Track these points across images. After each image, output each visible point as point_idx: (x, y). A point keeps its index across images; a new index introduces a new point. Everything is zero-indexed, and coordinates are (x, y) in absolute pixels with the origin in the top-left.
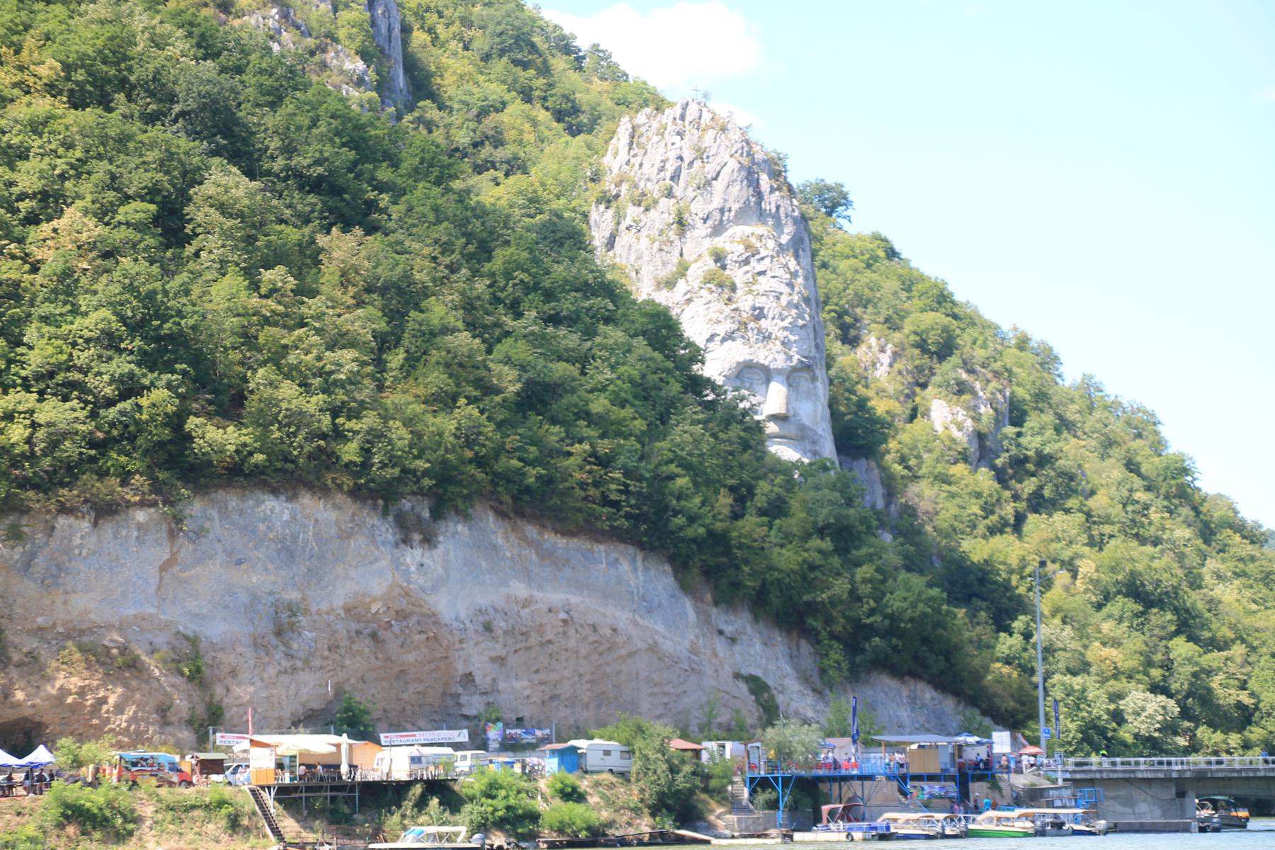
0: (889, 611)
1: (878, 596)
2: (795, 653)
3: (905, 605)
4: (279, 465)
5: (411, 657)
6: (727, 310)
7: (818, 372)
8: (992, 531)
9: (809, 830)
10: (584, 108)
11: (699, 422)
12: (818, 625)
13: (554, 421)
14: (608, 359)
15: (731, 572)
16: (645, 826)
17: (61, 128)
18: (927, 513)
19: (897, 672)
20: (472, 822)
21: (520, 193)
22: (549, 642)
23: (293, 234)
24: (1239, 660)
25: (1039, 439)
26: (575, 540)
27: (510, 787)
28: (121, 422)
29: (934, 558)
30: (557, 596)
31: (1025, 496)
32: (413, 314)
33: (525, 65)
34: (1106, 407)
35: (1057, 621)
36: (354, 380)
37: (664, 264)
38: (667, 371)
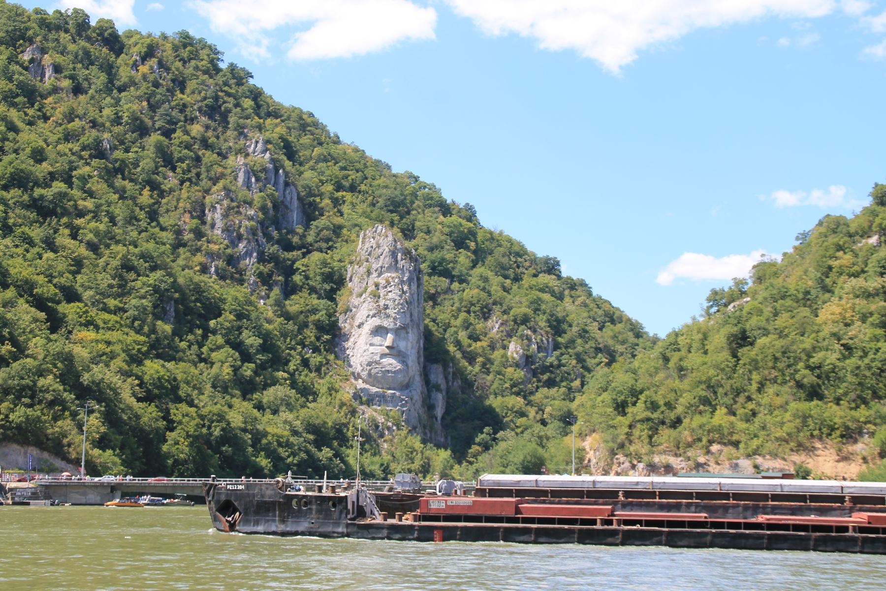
7: (410, 330)
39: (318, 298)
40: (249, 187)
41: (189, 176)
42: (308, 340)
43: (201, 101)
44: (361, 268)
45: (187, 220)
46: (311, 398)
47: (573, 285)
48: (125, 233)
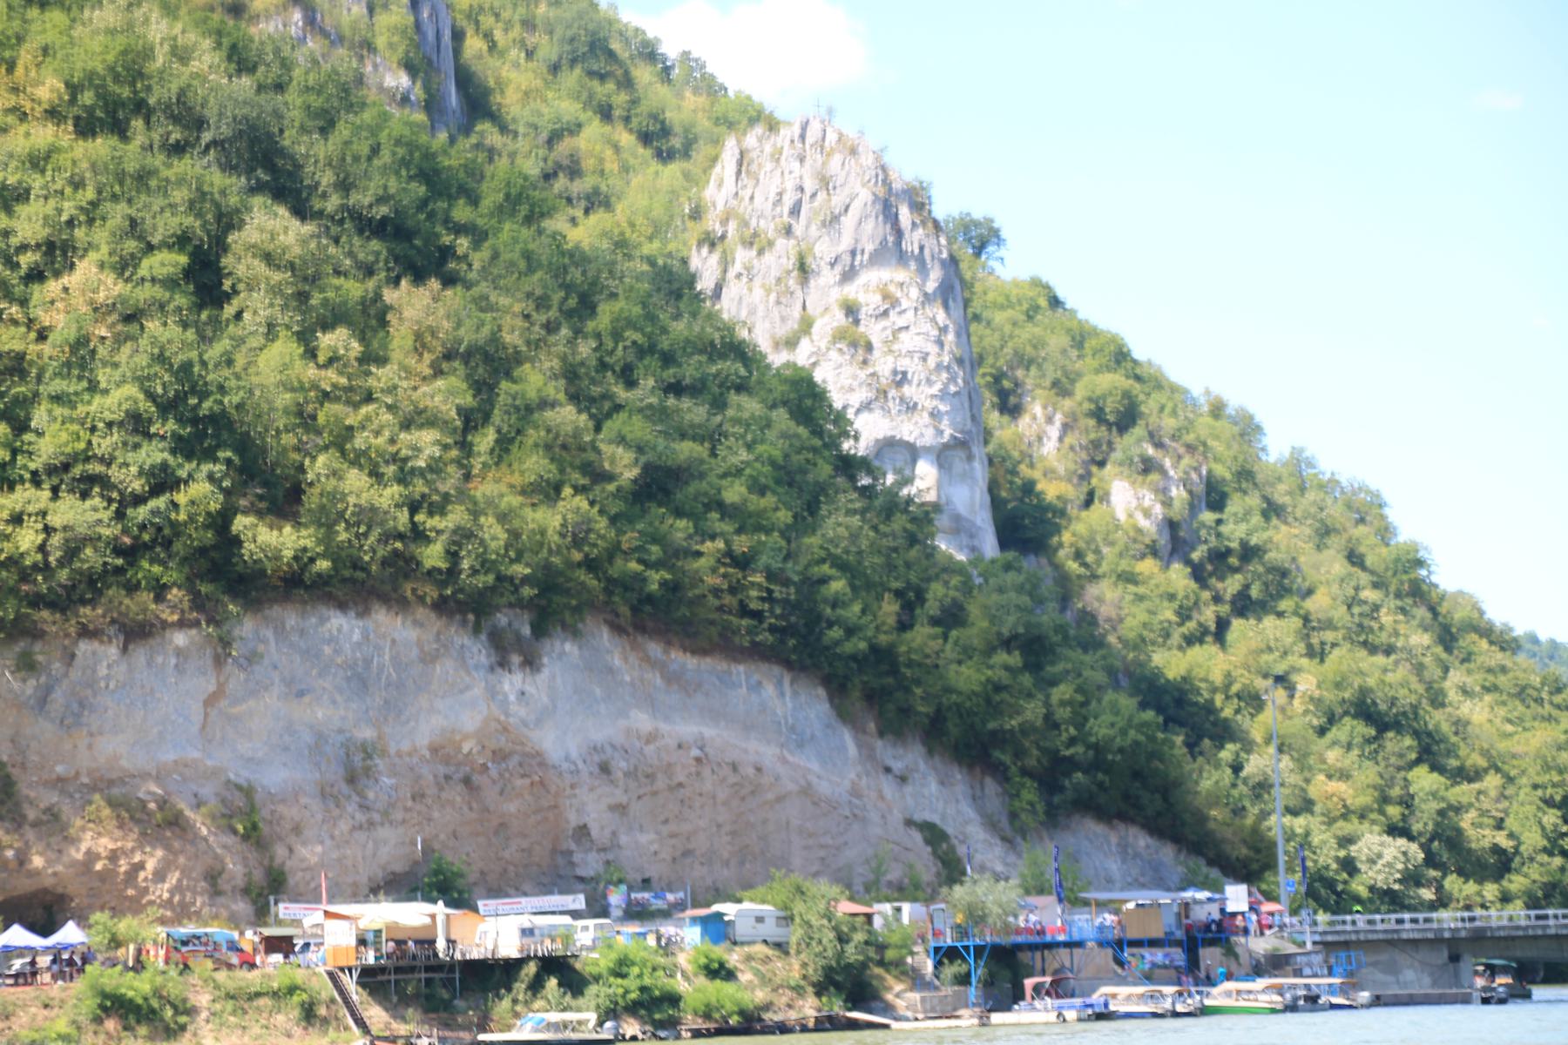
0: (1093, 739)
1: (1080, 721)
2: (978, 793)
3: (1111, 732)
4: (347, 573)
5: (512, 807)
6: (862, 374)
8: (1190, 640)
9: (1008, 1009)
10: (677, 129)
11: (855, 512)
12: (1006, 758)
13: (679, 513)
14: (743, 436)
15: (899, 695)
16: (809, 1008)
17: (69, 164)
18: (1109, 620)
19: (1105, 815)
20: (598, 1007)
21: (604, 234)
22: (680, 785)
23: (355, 289)
24: (1493, 793)
25: (1243, 527)
26: (708, 660)
27: (644, 963)
28: (152, 524)
29: (1120, 676)
30: (688, 729)
31: (1228, 597)
32: (504, 385)
33: (602, 77)
34: (1321, 486)
35: (1272, 750)
36: (435, 467)
37: (783, 319)
38: (814, 450)
44: (768, 257)
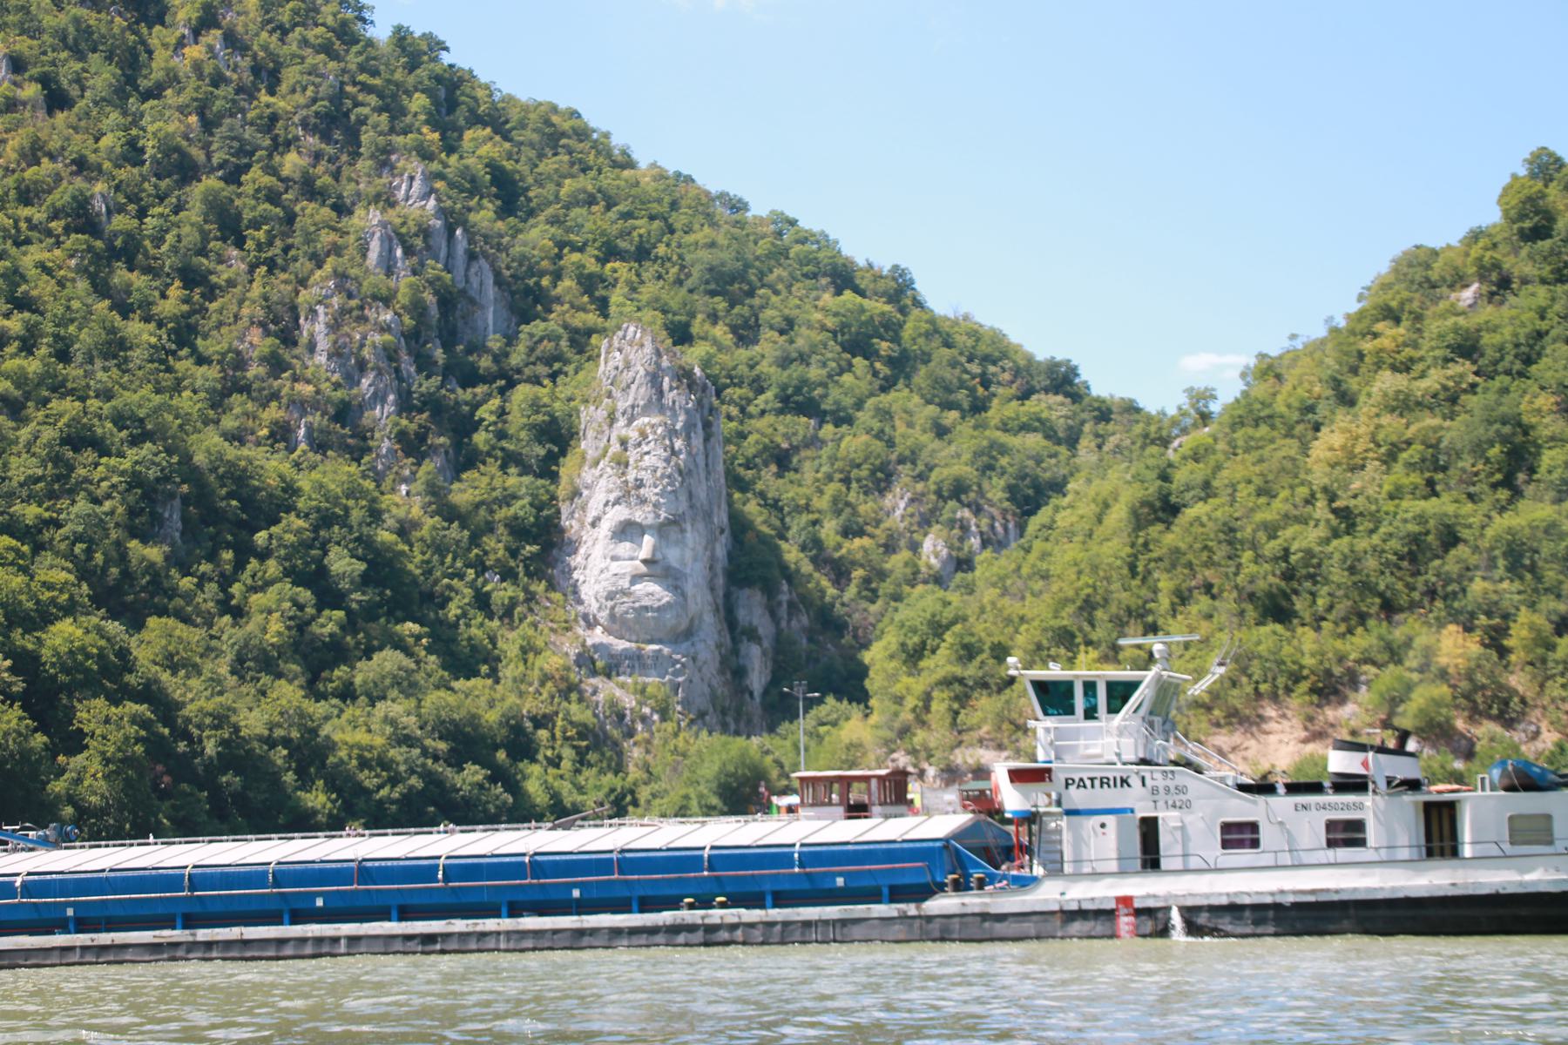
7: (688, 527)
39: (520, 475)
40: (389, 272)
41: (270, 254)
42: (492, 557)
43: (307, 106)
45: (256, 340)
46: (484, 669)
47: (1104, 413)
48: (87, 374)
